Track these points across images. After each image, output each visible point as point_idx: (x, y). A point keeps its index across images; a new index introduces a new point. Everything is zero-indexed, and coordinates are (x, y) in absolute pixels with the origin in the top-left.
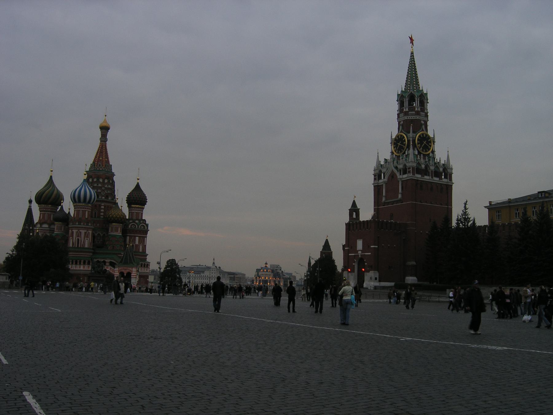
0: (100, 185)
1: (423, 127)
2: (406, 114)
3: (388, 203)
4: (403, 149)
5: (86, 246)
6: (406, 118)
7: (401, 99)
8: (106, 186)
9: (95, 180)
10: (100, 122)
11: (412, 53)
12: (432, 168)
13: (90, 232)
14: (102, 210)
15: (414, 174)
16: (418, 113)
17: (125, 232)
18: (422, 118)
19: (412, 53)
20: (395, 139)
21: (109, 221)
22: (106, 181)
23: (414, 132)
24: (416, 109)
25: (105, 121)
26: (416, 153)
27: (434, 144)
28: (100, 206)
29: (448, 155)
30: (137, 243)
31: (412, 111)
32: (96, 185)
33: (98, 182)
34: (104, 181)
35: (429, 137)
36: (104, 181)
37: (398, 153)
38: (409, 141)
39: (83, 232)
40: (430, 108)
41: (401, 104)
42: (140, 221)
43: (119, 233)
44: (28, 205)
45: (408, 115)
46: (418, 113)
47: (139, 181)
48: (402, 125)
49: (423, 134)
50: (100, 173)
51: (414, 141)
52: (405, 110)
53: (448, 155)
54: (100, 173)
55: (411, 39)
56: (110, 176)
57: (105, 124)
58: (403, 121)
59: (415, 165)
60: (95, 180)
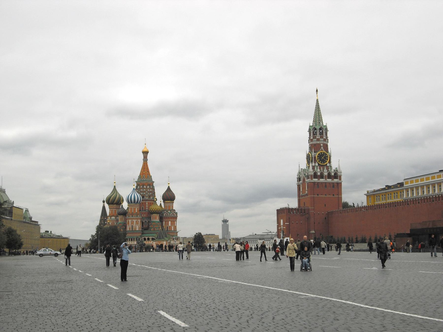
0: (144, 190)
1: (322, 148)
3: (302, 196)
5: (137, 230)
8: (148, 190)
9: (141, 187)
10: (142, 149)
11: (317, 100)
12: (326, 174)
13: (139, 221)
14: (147, 206)
15: (312, 179)
16: (318, 140)
17: (161, 219)
18: (321, 142)
21: (152, 213)
22: (148, 187)
23: (315, 152)
25: (145, 147)
26: (317, 165)
27: (330, 158)
28: (145, 203)
30: (170, 225)
31: (315, 138)
32: (142, 190)
33: (143, 188)
34: (147, 187)
36: (147, 187)
39: (135, 221)
40: (330, 135)
41: (310, 135)
42: (171, 211)
43: (158, 220)
44: (102, 204)
46: (318, 140)
47: (169, 185)
49: (321, 153)
50: (145, 182)
51: (315, 158)
54: (145, 182)
55: (317, 91)
56: (151, 184)
57: (145, 150)
59: (313, 173)
60: (141, 187)
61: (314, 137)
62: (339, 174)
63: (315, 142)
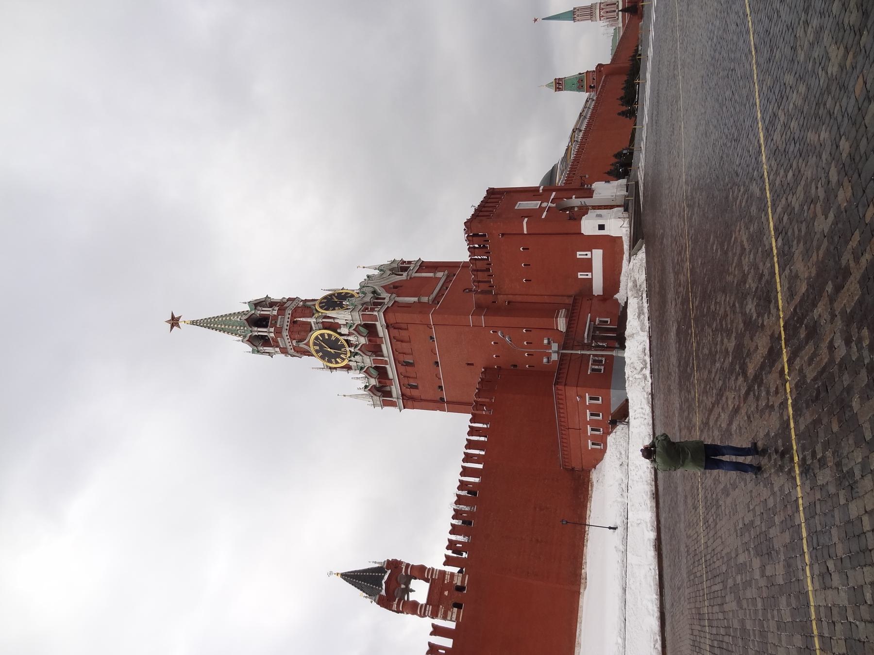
2: (278, 332)
4: (337, 340)
6: (285, 333)
7: (259, 343)
19: (194, 323)
20: (322, 358)
24: (275, 313)
29: (369, 268)
35: (331, 295)
38: (326, 326)
45: (281, 328)
48: (299, 341)
49: (321, 303)
52: (272, 335)
53: (369, 268)
58: (292, 339)
61: (274, 325)
62: (395, 265)
63: (285, 321)
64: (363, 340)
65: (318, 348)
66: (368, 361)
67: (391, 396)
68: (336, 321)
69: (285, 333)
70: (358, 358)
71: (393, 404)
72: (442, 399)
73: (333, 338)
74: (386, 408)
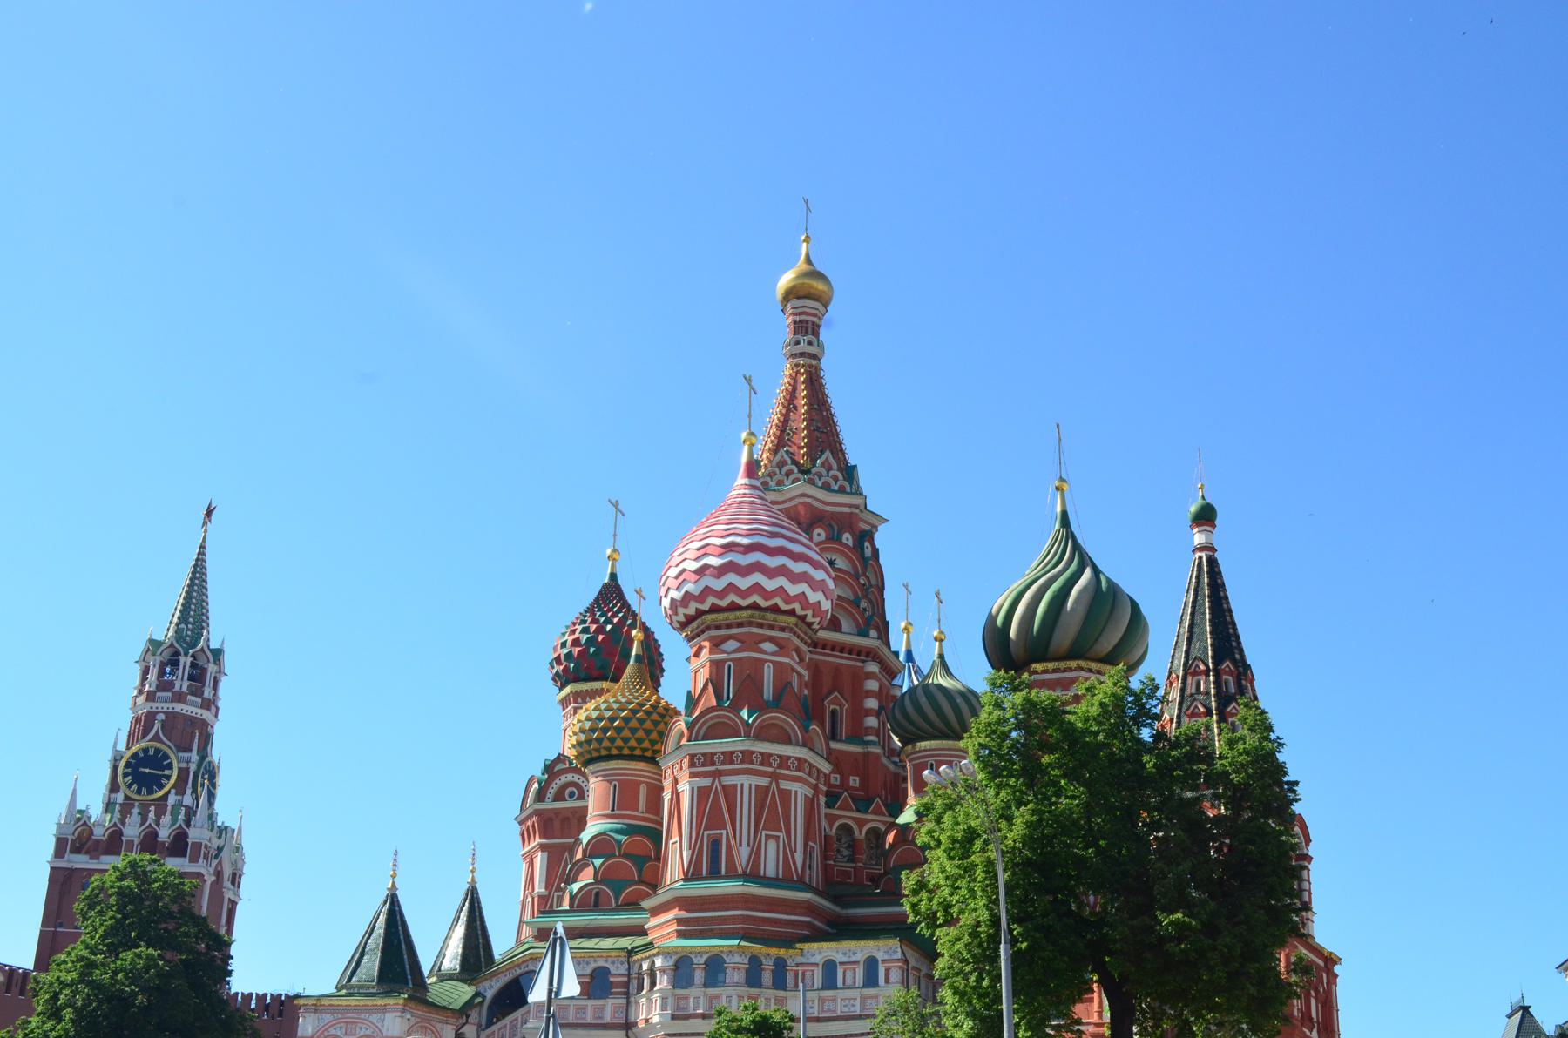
2: (179, 697)
6: (179, 707)
11: (203, 547)
19: (203, 547)
24: (208, 693)
37: (139, 792)
38: (183, 773)
45: (185, 702)
52: (177, 688)
55: (209, 513)
63: (190, 709)
64: (164, 834)
65: (151, 753)
66: (132, 831)
67: (72, 852)
68: (189, 791)
69: (179, 707)
70: (134, 818)
71: (60, 851)
72: (61, 925)
73: (164, 781)
74: (54, 840)
